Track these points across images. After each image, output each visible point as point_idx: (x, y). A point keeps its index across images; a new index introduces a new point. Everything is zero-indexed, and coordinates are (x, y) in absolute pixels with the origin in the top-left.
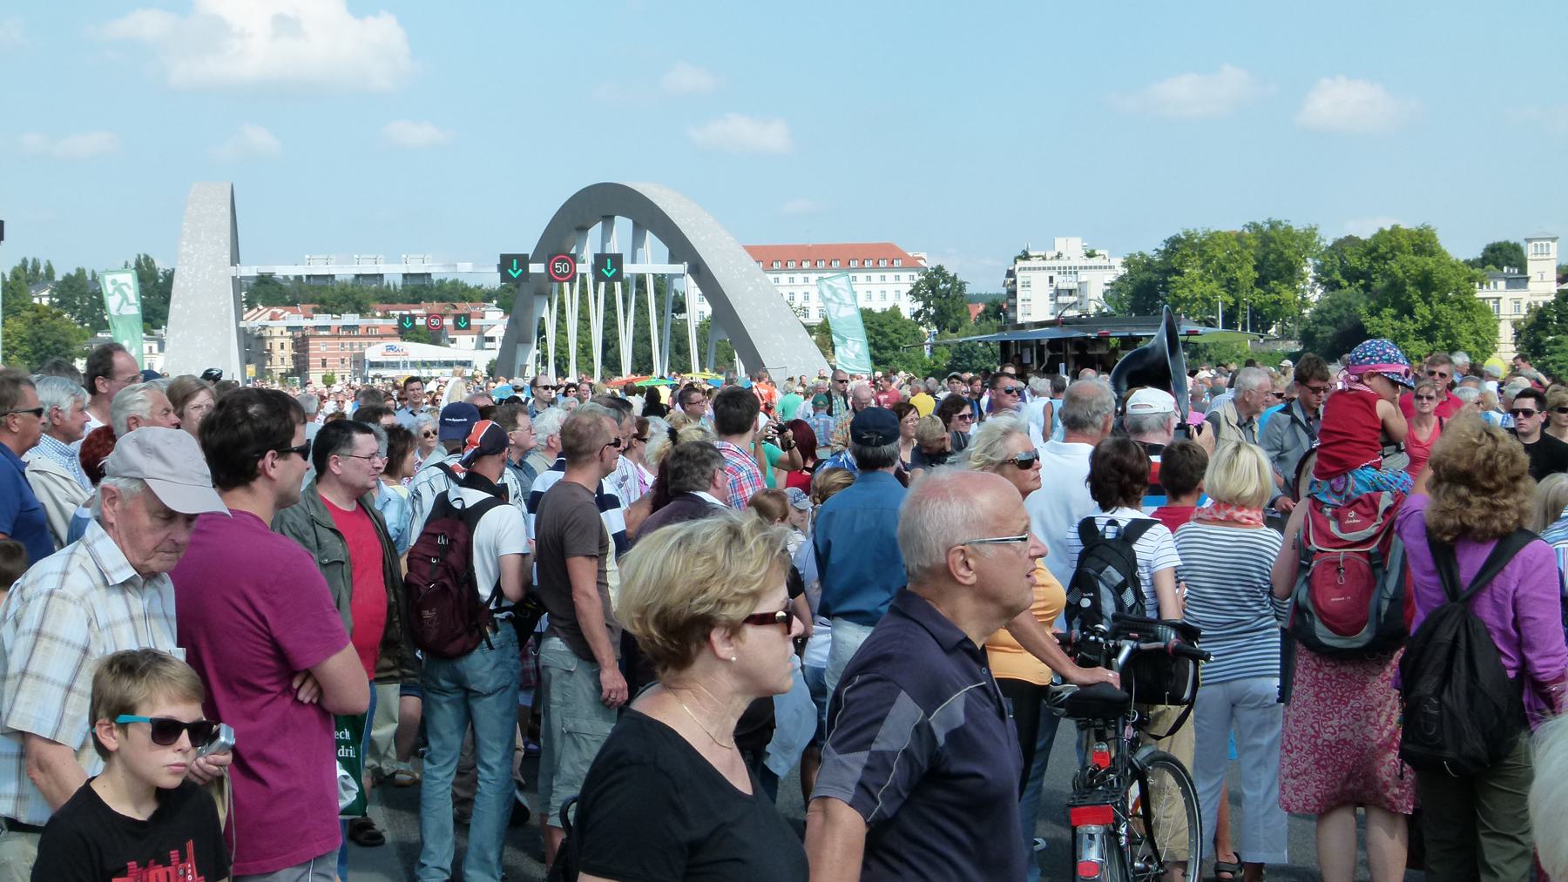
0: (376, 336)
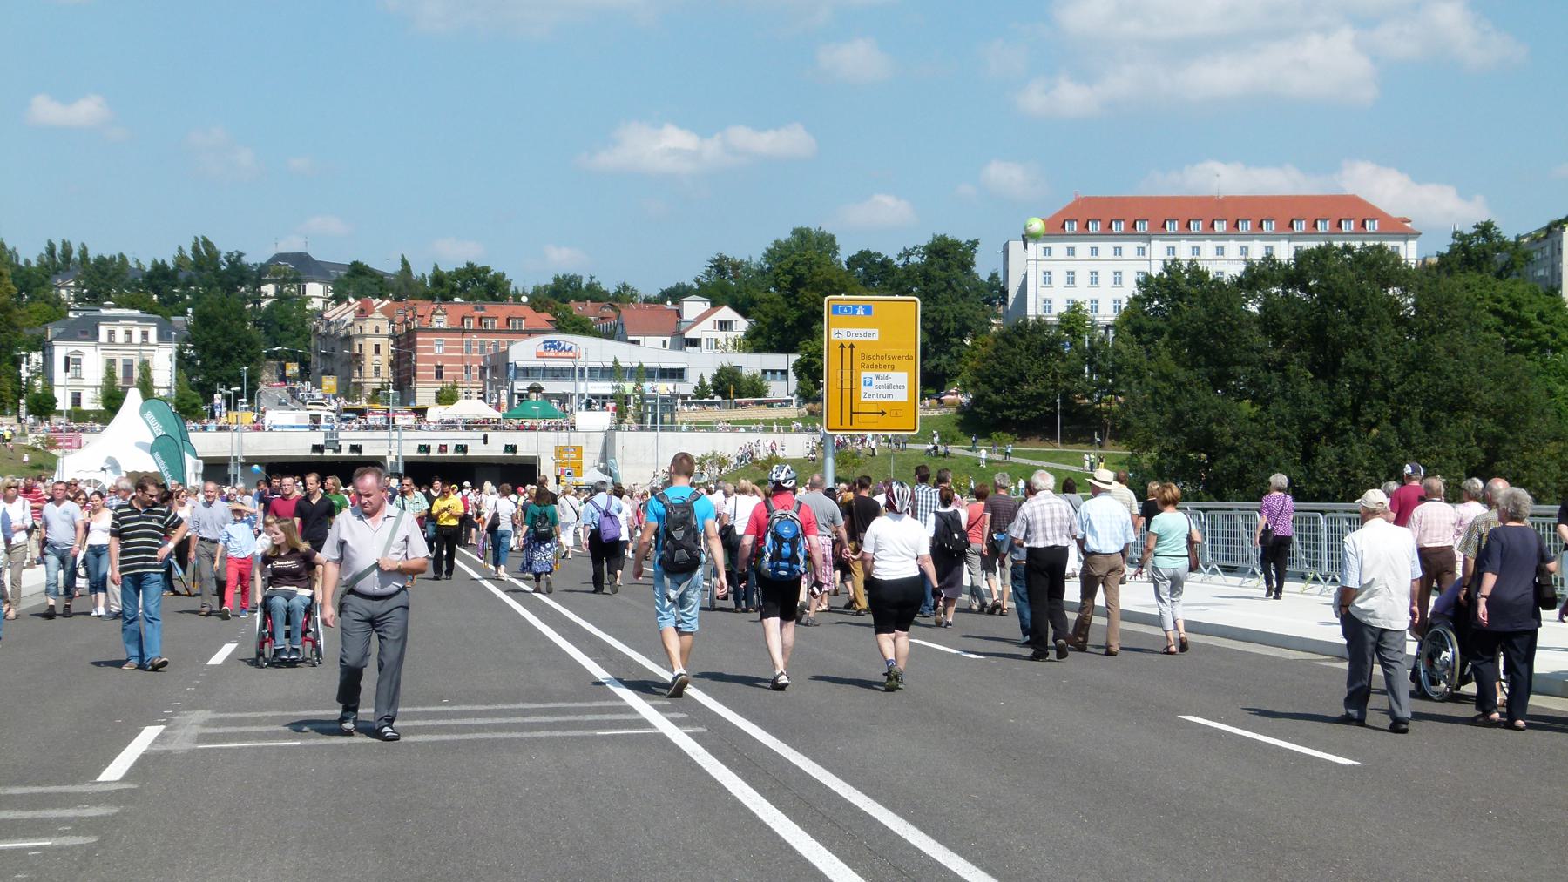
0: (521, 332)
